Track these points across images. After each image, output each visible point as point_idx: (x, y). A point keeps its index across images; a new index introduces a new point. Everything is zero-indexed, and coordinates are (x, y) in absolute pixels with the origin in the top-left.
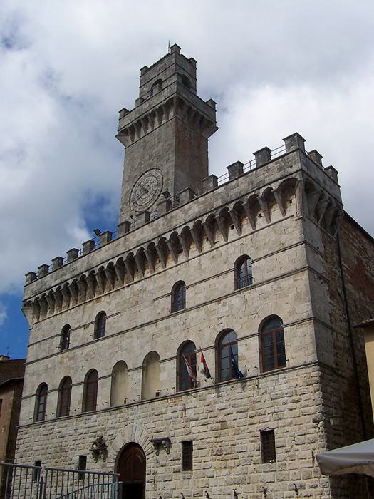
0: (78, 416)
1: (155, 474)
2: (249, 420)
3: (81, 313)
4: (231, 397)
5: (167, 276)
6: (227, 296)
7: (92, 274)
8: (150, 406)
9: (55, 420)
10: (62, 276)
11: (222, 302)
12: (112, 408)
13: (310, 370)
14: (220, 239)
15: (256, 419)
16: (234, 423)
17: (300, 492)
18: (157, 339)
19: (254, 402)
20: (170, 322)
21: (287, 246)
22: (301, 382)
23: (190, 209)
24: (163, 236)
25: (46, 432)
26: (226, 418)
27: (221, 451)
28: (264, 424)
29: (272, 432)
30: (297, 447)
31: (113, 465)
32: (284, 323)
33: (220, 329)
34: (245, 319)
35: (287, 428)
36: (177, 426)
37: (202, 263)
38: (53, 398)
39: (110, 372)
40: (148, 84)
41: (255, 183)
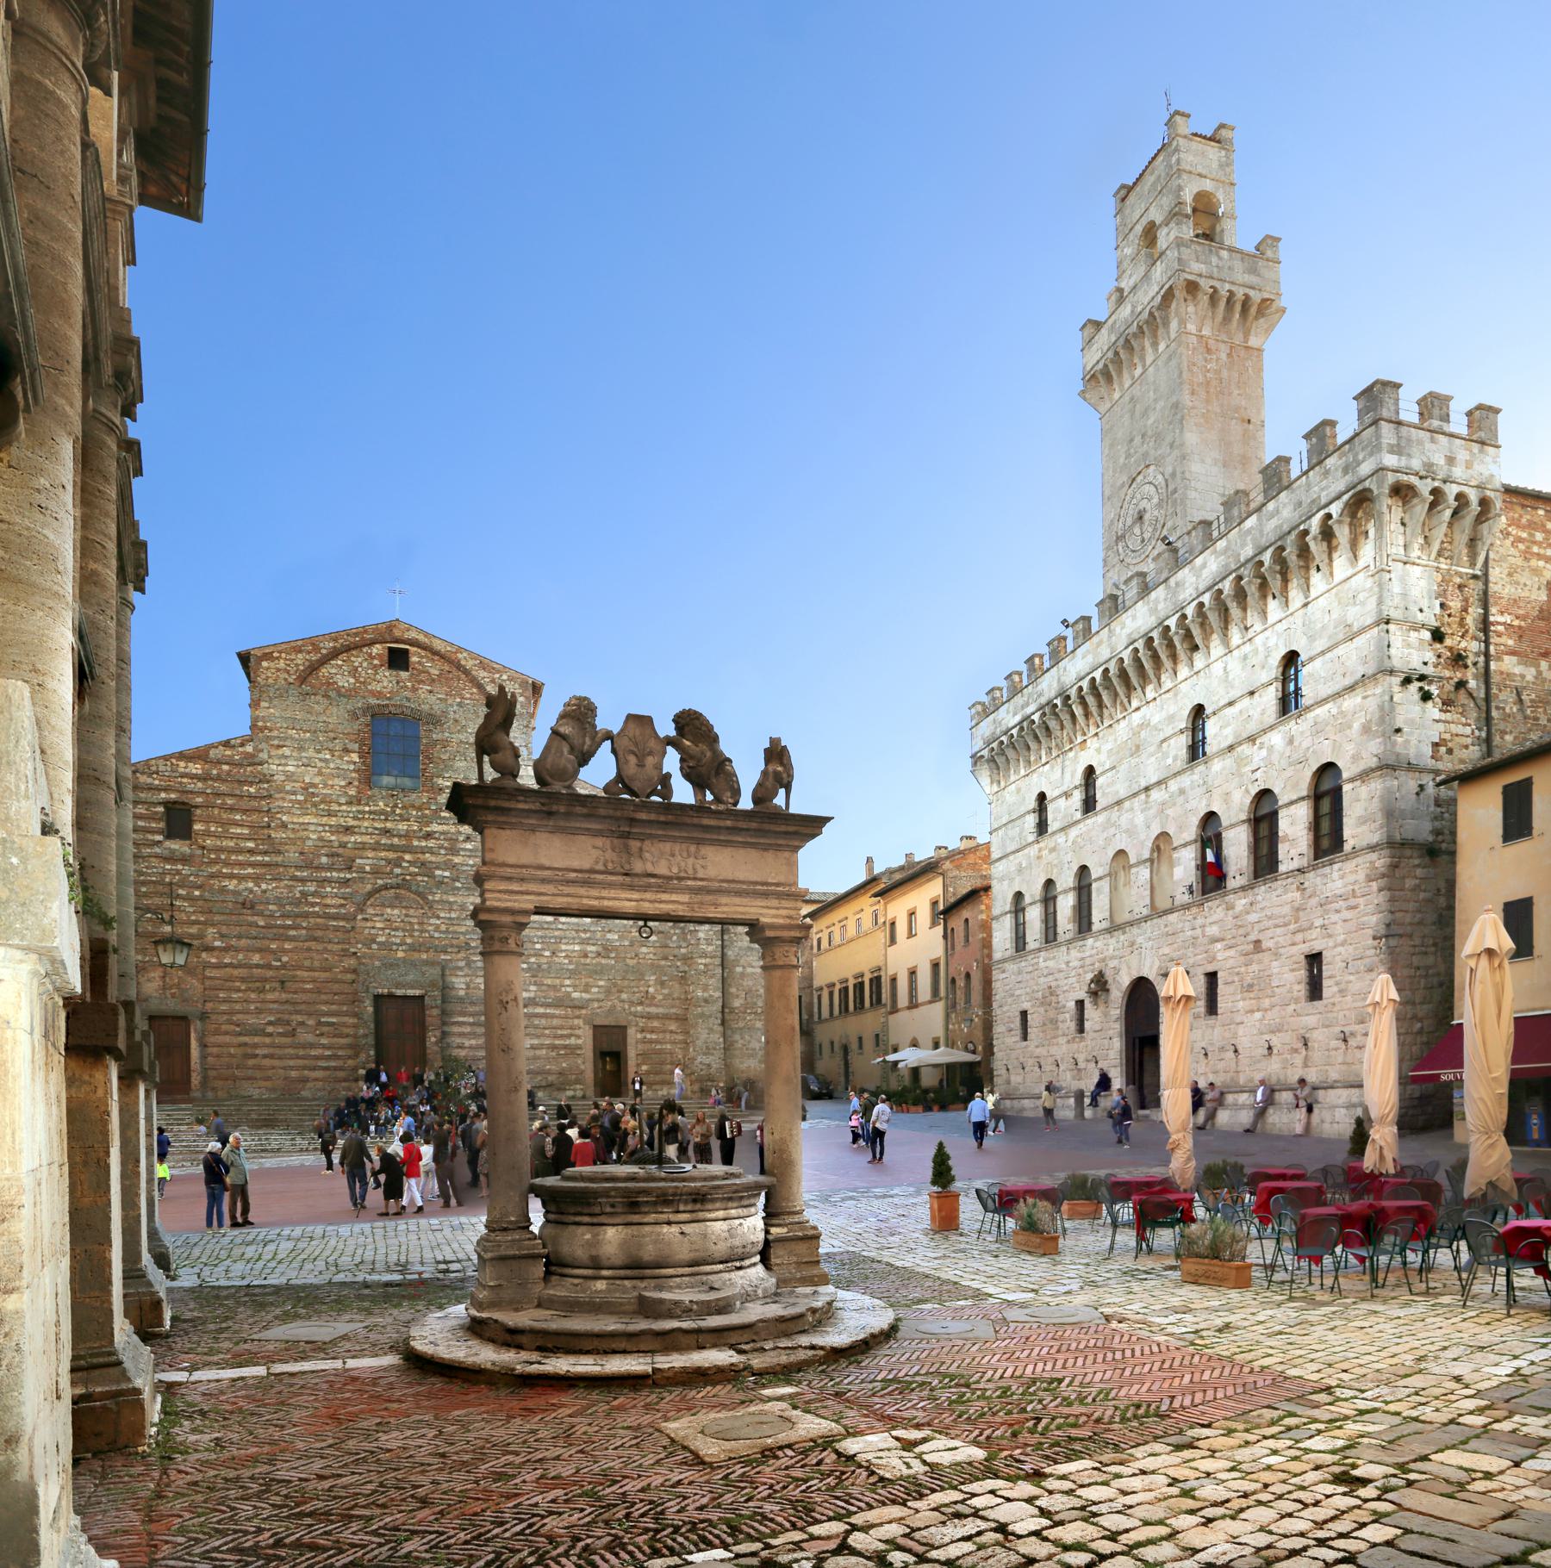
0: (1069, 942)
8: (1161, 921)
9: (1039, 950)
12: (1114, 928)
13: (1374, 856)
15: (1299, 937)
19: (1298, 909)
22: (1361, 876)
29: (1319, 954)
32: (1345, 775)
33: (1254, 790)
35: (1340, 949)
38: (1034, 915)
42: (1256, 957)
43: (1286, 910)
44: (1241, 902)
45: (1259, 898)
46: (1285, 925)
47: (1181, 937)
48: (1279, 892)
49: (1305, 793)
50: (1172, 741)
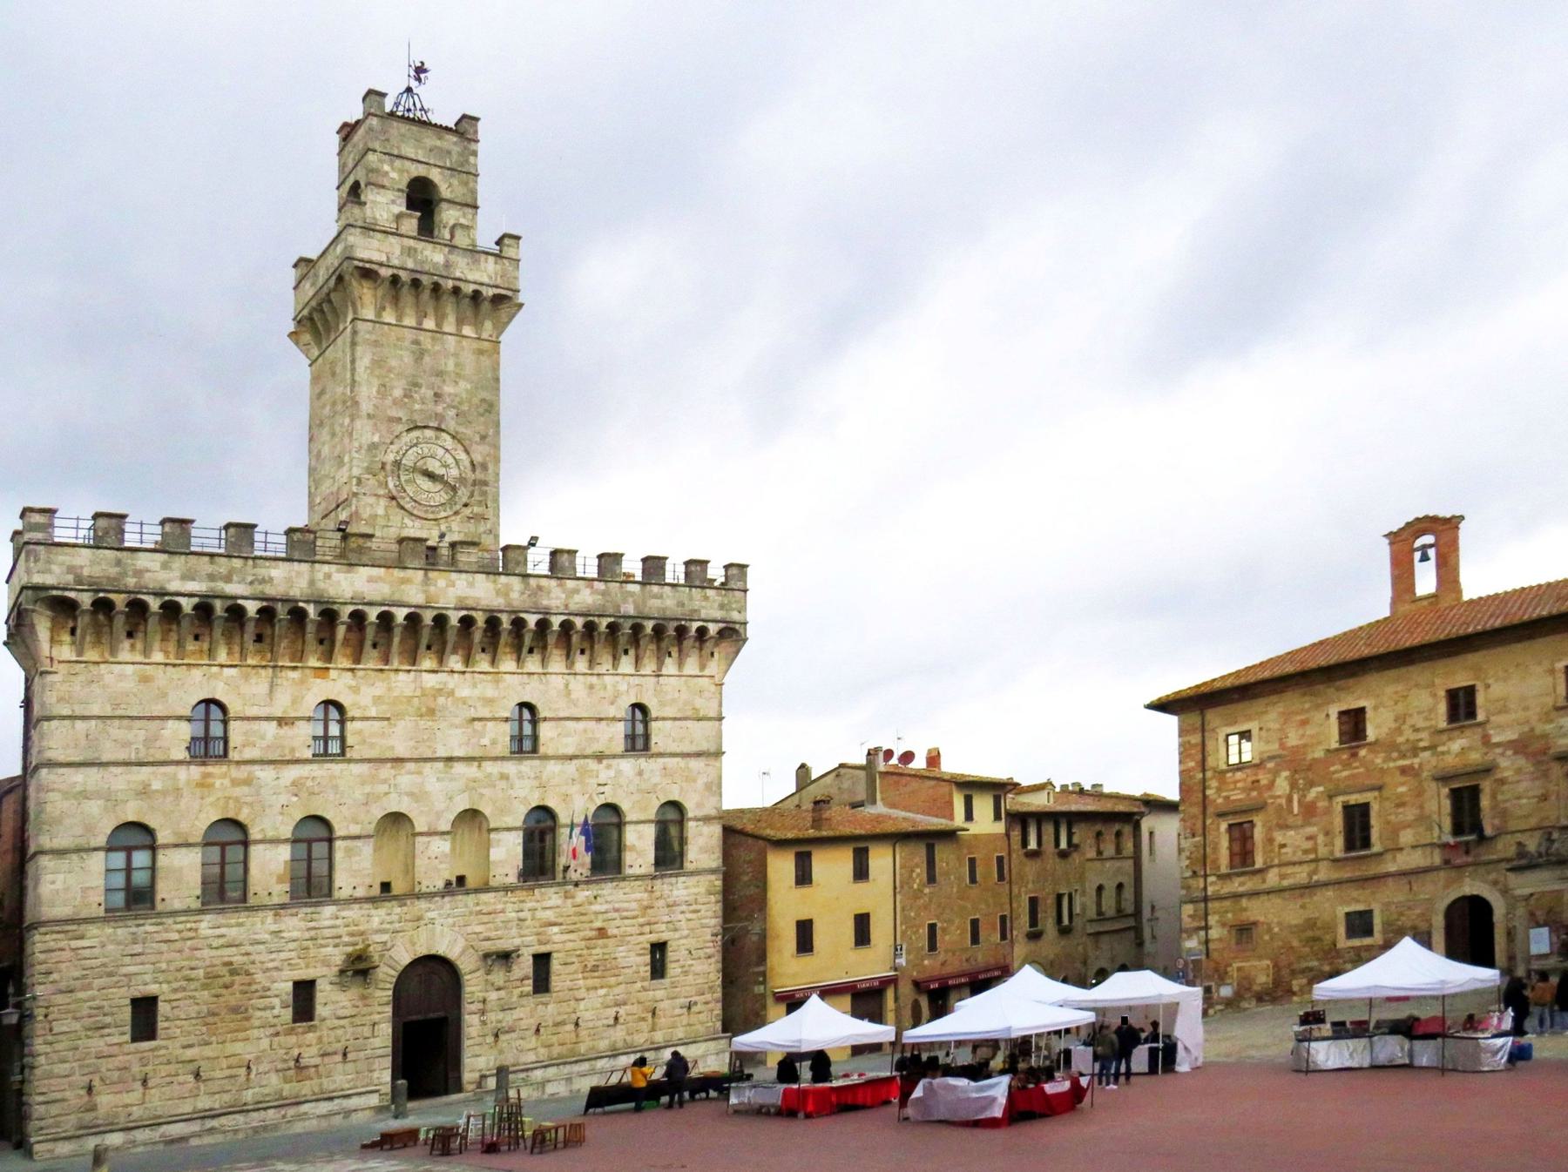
1: (484, 1001)
2: (635, 930)
5: (501, 686)
8: (471, 899)
13: (713, 877)
14: (605, 665)
15: (647, 929)
16: (615, 931)
17: (694, 1009)
18: (484, 791)
19: (647, 908)
20: (510, 768)
22: (702, 890)
23: (577, 591)
33: (600, 801)
34: (636, 797)
37: (571, 687)
39: (370, 829)
42: (600, 942)
43: (634, 905)
44: (583, 894)
46: (634, 917)
50: (490, 724)
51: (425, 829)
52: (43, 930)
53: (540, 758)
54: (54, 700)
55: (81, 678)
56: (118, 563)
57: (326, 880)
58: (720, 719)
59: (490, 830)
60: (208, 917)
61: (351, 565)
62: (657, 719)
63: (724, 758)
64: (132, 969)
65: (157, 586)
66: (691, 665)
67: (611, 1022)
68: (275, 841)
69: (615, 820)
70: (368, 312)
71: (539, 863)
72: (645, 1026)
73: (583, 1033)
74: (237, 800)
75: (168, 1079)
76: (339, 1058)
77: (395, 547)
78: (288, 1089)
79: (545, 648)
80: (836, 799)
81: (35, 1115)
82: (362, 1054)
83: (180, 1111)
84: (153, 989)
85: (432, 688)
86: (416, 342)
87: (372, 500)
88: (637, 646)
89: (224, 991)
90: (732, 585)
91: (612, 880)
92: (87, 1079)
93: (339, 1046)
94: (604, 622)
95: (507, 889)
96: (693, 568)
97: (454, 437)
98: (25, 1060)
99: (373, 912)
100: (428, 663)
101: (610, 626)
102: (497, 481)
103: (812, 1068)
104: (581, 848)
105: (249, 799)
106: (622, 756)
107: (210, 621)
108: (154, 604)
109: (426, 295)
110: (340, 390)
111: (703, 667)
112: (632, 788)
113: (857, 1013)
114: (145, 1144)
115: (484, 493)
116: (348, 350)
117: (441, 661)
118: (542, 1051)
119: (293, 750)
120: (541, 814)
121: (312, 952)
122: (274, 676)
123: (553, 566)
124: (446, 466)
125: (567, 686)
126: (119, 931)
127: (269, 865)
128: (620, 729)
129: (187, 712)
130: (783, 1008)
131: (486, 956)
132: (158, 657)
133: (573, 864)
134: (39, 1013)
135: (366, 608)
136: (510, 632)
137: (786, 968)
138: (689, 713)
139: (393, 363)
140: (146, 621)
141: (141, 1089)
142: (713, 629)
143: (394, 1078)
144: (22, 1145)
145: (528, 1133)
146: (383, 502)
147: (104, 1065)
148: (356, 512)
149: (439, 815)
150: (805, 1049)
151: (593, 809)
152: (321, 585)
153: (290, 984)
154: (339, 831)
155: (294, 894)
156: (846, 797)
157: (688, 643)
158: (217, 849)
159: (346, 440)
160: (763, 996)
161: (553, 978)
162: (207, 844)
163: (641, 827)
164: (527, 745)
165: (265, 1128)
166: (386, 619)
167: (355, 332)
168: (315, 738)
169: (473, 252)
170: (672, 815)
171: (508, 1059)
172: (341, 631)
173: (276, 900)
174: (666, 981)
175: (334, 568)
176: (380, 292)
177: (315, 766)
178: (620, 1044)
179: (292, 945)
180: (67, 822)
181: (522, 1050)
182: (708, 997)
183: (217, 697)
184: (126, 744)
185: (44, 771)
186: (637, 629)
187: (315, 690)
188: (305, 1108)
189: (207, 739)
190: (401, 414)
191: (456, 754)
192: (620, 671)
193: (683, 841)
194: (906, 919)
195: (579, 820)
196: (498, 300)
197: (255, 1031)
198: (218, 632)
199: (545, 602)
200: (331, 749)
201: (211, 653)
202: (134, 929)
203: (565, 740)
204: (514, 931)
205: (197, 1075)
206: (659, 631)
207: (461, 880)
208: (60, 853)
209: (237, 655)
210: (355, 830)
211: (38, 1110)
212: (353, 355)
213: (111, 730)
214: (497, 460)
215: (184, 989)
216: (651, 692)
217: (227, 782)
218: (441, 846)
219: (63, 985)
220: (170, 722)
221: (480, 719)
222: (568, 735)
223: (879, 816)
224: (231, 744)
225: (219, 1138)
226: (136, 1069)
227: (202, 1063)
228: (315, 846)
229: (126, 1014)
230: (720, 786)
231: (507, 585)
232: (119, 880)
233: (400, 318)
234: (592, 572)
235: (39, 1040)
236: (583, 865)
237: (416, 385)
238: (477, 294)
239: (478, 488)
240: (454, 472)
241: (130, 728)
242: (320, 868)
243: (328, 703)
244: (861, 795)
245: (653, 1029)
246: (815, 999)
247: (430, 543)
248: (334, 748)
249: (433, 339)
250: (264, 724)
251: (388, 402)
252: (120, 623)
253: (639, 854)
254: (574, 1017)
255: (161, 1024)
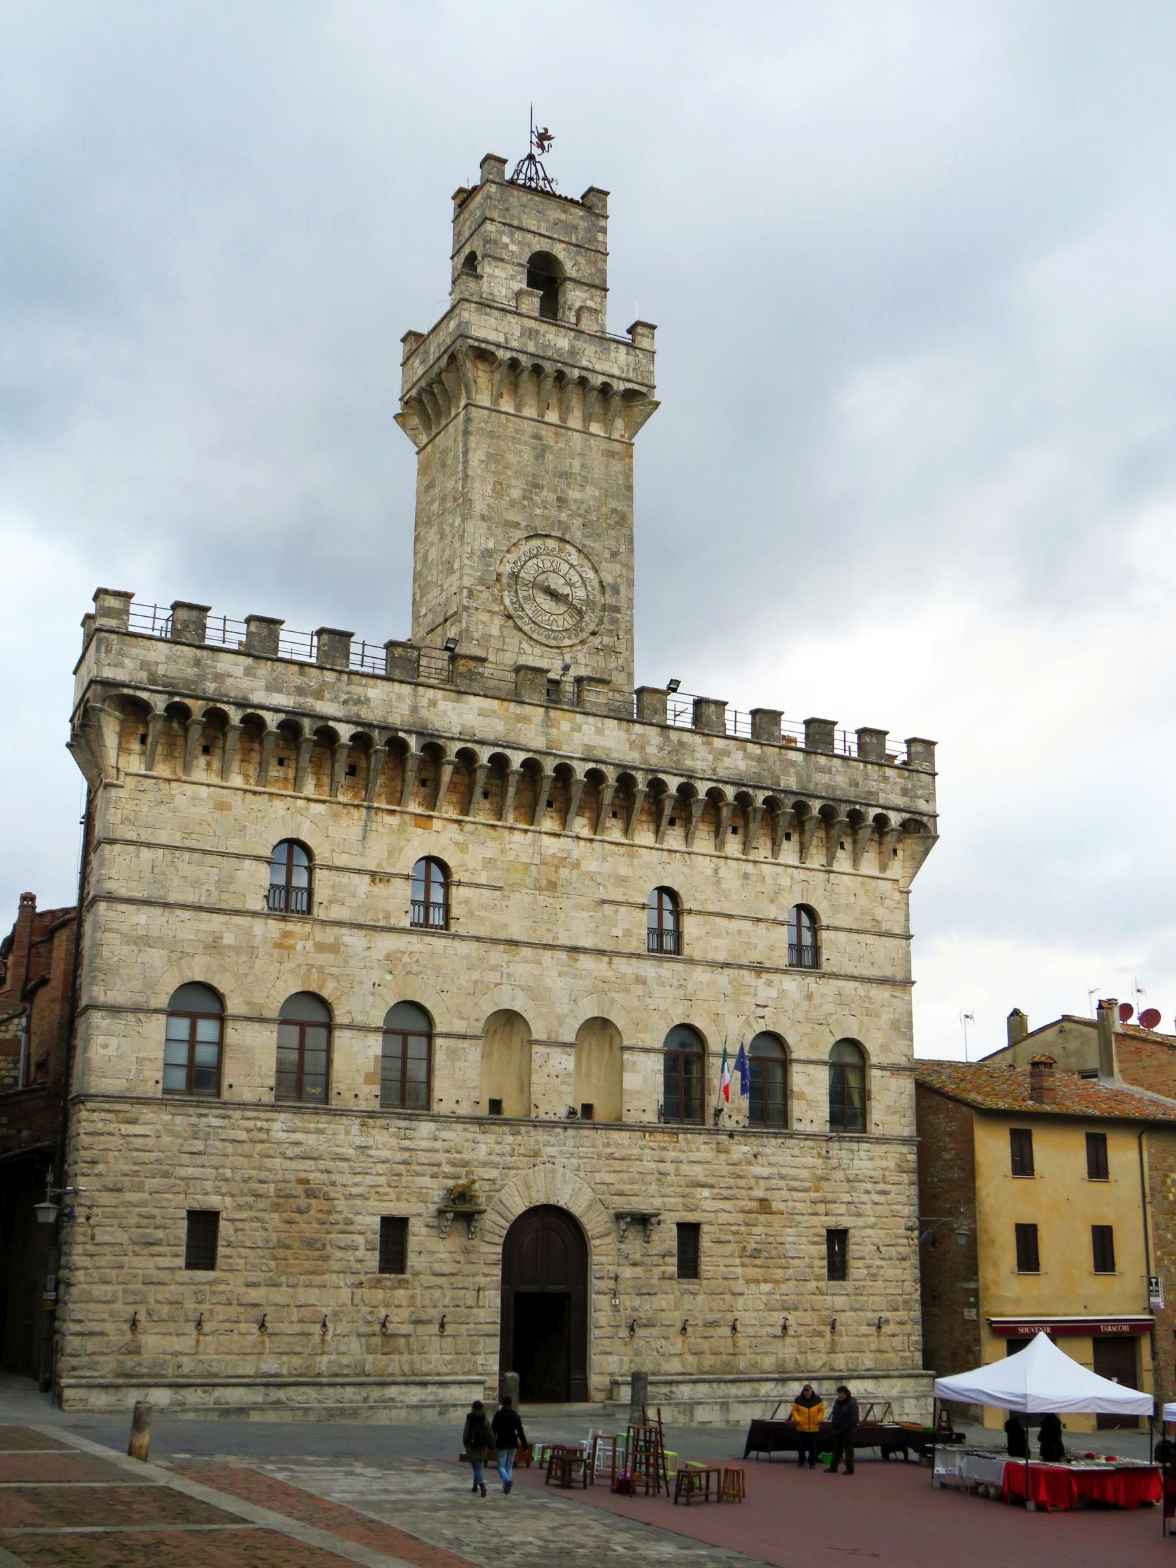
1: (616, 1278)
3: (355, 832)
4: (779, 1160)
5: (636, 861)
6: (777, 970)
7: (433, 751)
8: (599, 1136)
10: (300, 691)
11: (764, 976)
13: (905, 1149)
14: (763, 850)
15: (821, 1208)
16: (781, 1206)
17: (885, 1329)
18: (615, 996)
19: (822, 1179)
21: (884, 929)
22: (892, 1165)
23: (727, 753)
24: (660, 776)
25: (232, 1134)
26: (768, 1195)
27: (760, 1251)
28: (834, 1219)
30: (882, 1263)
31: (499, 1249)
33: (760, 1027)
34: (807, 1028)
35: (869, 1232)
36: (669, 1190)
37: (722, 873)
39: (477, 1028)
40: (518, 235)
41: (860, 789)
42: (762, 1218)
44: (740, 1149)
45: (767, 1150)
47: (636, 1166)
48: (796, 1152)
49: (826, 1058)
50: (623, 910)
51: (542, 1036)
52: (89, 1105)
53: (684, 961)
54: (118, 820)
55: (150, 796)
56: (197, 663)
57: (424, 1086)
58: (909, 937)
59: (624, 1049)
60: (282, 1116)
61: (459, 692)
62: (828, 928)
63: (914, 988)
64: (190, 1172)
65: (240, 695)
66: (869, 864)
67: (779, 1332)
68: (366, 1029)
69: (778, 1055)
70: (484, 399)
71: (684, 1101)
72: (822, 1343)
73: (743, 1342)
74: (321, 969)
75: (228, 1325)
76: (434, 1328)
77: (511, 676)
78: (371, 1362)
79: (688, 821)
80: (1060, 1065)
81: (68, 1350)
82: (463, 1328)
83: (240, 1372)
84: (213, 1201)
85: (553, 856)
86: (538, 437)
87: (485, 617)
88: (802, 833)
89: (297, 1217)
90: (916, 765)
91: (776, 1136)
92: (131, 1309)
93: (435, 1313)
94: (760, 796)
95: (645, 1129)
96: (867, 739)
97: (580, 551)
98: (64, 1273)
99: (479, 1137)
100: (549, 823)
101: (766, 801)
102: (631, 608)
103: (1041, 1438)
104: (736, 1087)
105: (334, 971)
106: (785, 972)
107: (295, 745)
108: (235, 716)
109: (549, 383)
110: (450, 484)
111: (883, 867)
112: (800, 1016)
113: (1103, 1369)
114: (197, 1410)
115: (614, 621)
116: (459, 439)
117: (564, 823)
118: (690, 1358)
119: (387, 916)
120: (687, 1036)
121: (405, 1179)
122: (368, 820)
123: (697, 718)
124: (570, 584)
125: (716, 871)
126: (178, 1119)
127: (357, 1058)
128: (782, 937)
129: (267, 852)
130: (1002, 1345)
131: (619, 1217)
132: (237, 780)
133: (727, 1107)
134: (79, 1211)
135: (477, 748)
136: (647, 796)
137: (1006, 1291)
138: (868, 926)
139: (511, 458)
140: (225, 735)
141: (194, 1333)
142: (895, 819)
143: (503, 1368)
144: (50, 1388)
145: (671, 1474)
146: (498, 621)
147: (155, 1294)
148: (467, 630)
149: (561, 1019)
150: (1032, 1408)
151: (750, 1037)
152: (424, 713)
153: (378, 1219)
154: (440, 1028)
155: (384, 1098)
156: (1073, 1062)
157: (865, 833)
158: (295, 1030)
159: (457, 544)
160: (975, 1324)
161: (703, 1259)
162: (284, 1022)
163: (811, 1068)
164: (668, 943)
165: (342, 1412)
166: (499, 763)
167: (468, 420)
168: (414, 902)
169: (603, 339)
170: (850, 1058)
171: (648, 1367)
172: (447, 772)
173: (363, 1106)
174: (848, 1285)
175: (440, 693)
176: (497, 376)
177: (414, 939)
178: (790, 1365)
179: (381, 1168)
180: (125, 972)
181: (666, 1355)
182: (902, 1314)
183: (302, 838)
184: (196, 884)
185: (102, 906)
186: (801, 808)
187: (416, 841)
188: (392, 1391)
189: (288, 888)
190: (518, 519)
191: (581, 944)
192: (780, 861)
193: (865, 1095)
194: (1161, 1243)
195: (734, 1049)
196: (631, 396)
197: (334, 1276)
198: (305, 757)
199: (688, 763)
200: (433, 915)
201: (297, 783)
202: (194, 1120)
203: (716, 942)
204: (654, 1187)
205: (262, 1326)
206: (828, 814)
207: (588, 1109)
208: (115, 1010)
209: (326, 789)
210: (459, 1027)
211: (72, 1343)
212: (465, 444)
213: (180, 865)
214: (631, 584)
215: (251, 1208)
216: (820, 891)
217: (309, 944)
218: (563, 1061)
219: (109, 1181)
220: (247, 862)
221: (611, 902)
222: (718, 936)
223: (1118, 1093)
224: (317, 899)
225: (285, 1417)
226: (190, 1305)
227: (269, 1310)
228: (411, 1039)
229: (181, 1229)
230: (910, 1026)
231: (642, 735)
232: (180, 1054)
233: (519, 407)
234: (745, 731)
235: (78, 1249)
236: (739, 1111)
237: (536, 486)
238: (605, 384)
239: (606, 616)
240: (580, 593)
241: (201, 864)
242: (417, 1070)
243: (430, 860)
244: (1093, 1063)
245: (832, 1351)
246: (1042, 1339)
247: (551, 675)
248: (436, 917)
249: (557, 435)
250: (356, 878)
251: (504, 503)
252: (196, 733)
253: (811, 1104)
254: (730, 1317)
255: (222, 1250)
